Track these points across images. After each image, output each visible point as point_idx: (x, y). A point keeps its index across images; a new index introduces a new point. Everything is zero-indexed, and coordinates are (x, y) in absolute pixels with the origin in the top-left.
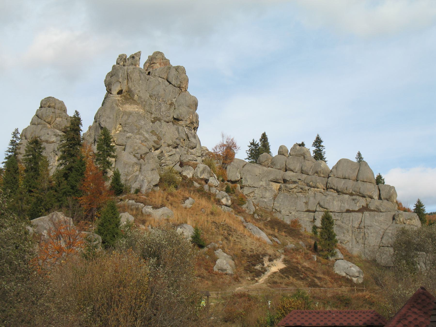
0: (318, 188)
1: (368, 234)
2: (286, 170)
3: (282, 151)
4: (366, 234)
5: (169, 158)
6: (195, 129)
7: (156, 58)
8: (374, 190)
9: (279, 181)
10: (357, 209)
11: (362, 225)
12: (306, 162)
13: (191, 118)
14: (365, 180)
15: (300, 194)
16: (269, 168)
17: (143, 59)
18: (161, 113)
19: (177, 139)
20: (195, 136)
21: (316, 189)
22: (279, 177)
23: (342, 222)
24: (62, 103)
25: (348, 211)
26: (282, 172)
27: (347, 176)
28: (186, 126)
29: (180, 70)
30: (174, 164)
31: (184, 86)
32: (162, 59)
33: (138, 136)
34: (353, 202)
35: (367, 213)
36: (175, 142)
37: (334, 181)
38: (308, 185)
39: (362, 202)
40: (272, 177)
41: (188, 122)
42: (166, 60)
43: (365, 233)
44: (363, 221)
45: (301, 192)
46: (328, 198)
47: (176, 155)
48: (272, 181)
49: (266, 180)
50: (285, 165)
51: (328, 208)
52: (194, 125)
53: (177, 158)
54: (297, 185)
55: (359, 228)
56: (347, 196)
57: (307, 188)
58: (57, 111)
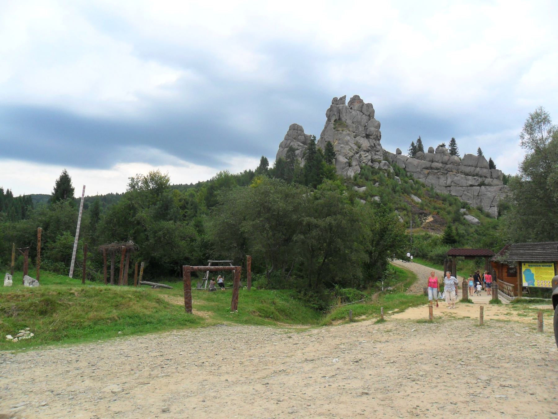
3: (431, 150)
6: (379, 140)
7: (356, 99)
11: (480, 194)
15: (441, 176)
17: (347, 100)
20: (379, 145)
22: (428, 165)
24: (301, 127)
25: (471, 186)
29: (370, 106)
33: (347, 146)
35: (483, 187)
37: (462, 168)
38: (446, 170)
39: (480, 180)
40: (424, 166)
46: (459, 178)
52: (378, 138)
53: (370, 157)
55: (478, 196)
58: (299, 132)
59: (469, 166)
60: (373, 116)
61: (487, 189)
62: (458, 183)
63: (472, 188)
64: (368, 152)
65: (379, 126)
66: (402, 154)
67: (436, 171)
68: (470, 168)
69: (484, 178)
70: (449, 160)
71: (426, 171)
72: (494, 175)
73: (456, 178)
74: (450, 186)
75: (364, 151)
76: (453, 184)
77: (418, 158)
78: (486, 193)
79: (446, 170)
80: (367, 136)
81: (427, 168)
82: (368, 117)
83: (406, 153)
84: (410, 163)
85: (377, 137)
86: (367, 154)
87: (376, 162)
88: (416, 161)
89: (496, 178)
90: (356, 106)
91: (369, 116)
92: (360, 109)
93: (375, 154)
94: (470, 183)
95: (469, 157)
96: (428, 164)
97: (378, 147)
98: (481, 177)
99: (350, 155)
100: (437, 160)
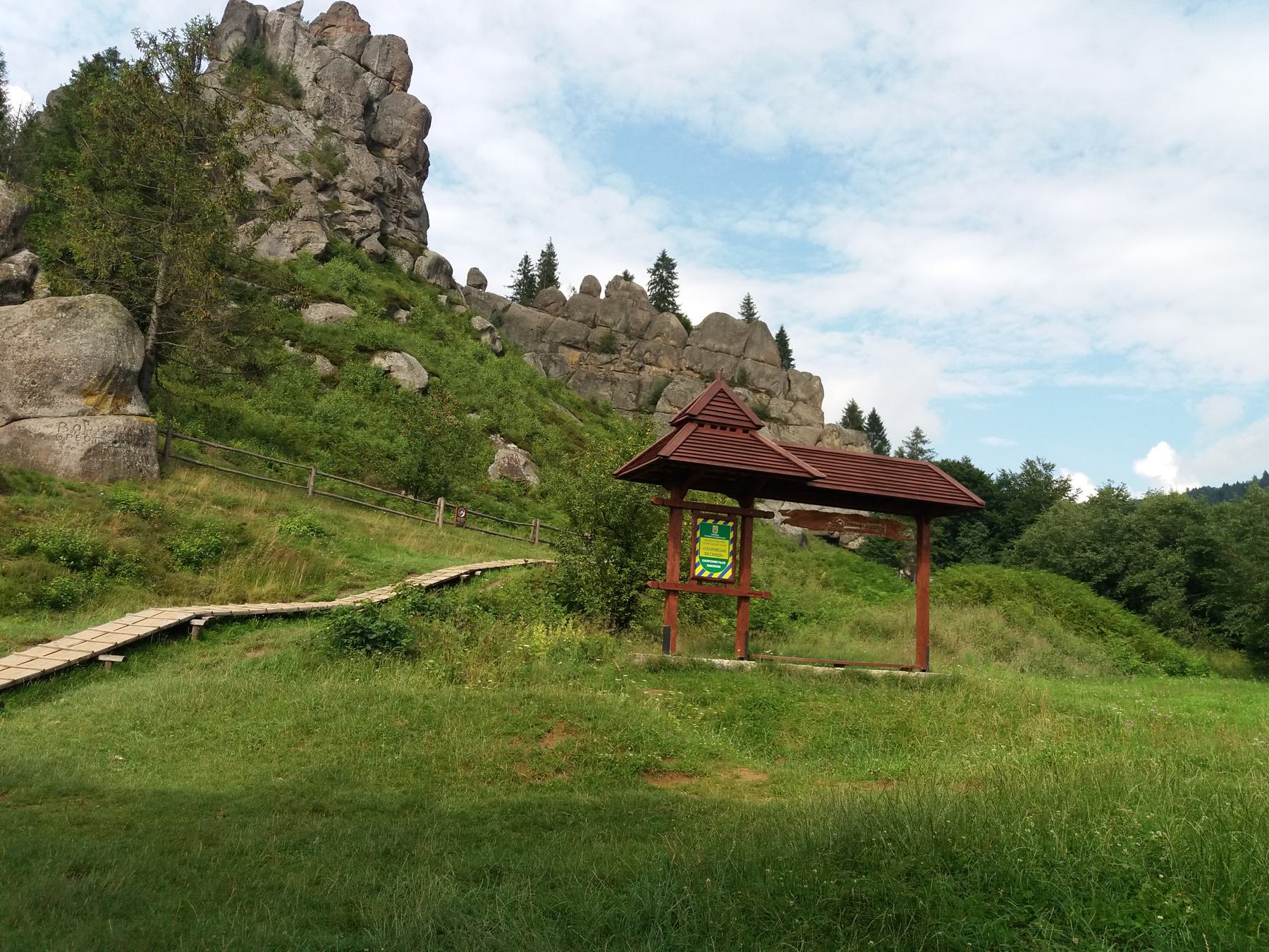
0: (660, 366)
2: (594, 326)
3: (590, 286)
5: (353, 217)
9: (579, 345)
16: (560, 319)
18: (342, 120)
19: (377, 179)
21: (654, 368)
29: (395, 46)
30: (363, 235)
41: (407, 154)
45: (623, 371)
48: (563, 344)
53: (374, 220)
60: (405, 85)
64: (370, 199)
65: (425, 120)
67: (605, 358)
68: (719, 357)
70: (649, 324)
71: (573, 356)
72: (798, 392)
77: (543, 308)
80: (374, 146)
83: (502, 284)
86: (366, 206)
87: (402, 247)
89: (804, 401)
91: (389, 78)
92: (352, 52)
95: (718, 321)
96: (580, 332)
97: (413, 198)
98: (756, 391)
99: (284, 176)
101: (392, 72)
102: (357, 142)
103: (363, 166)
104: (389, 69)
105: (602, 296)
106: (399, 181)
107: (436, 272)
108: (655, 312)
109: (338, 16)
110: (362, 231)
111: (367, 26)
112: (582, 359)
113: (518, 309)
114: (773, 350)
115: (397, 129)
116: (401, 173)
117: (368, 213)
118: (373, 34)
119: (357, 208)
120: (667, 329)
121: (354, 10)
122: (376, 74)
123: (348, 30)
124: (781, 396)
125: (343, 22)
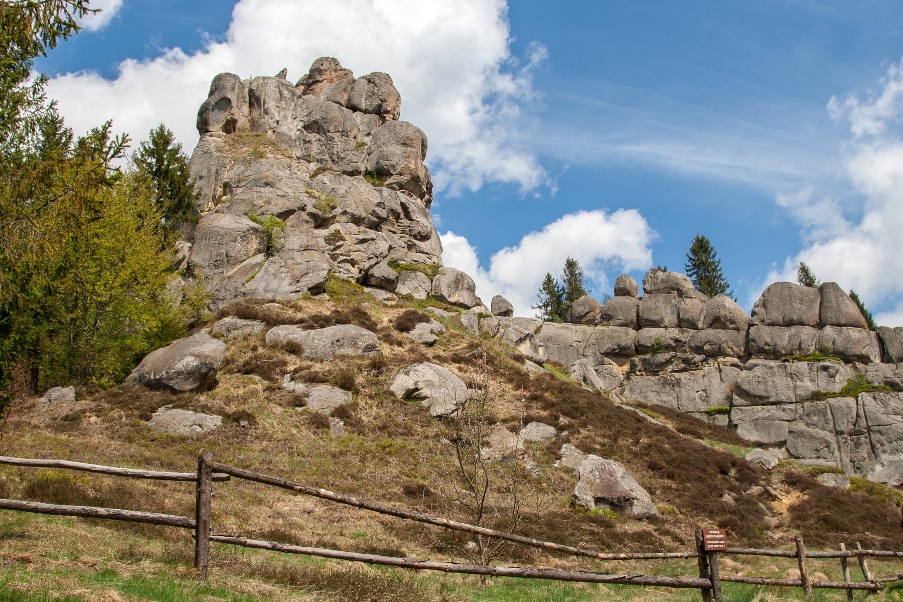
1: (882, 445)
4: (878, 446)
8: (868, 342)
10: (838, 387)
11: (863, 423)
12: (688, 300)
13: (413, 167)
14: (843, 321)
16: (599, 327)
19: (379, 205)
21: (721, 359)
23: (808, 425)
26: (632, 332)
27: (795, 317)
28: (401, 187)
31: (389, 109)
32: (336, 71)
34: (825, 373)
35: (866, 398)
36: (374, 211)
37: (765, 335)
38: (698, 350)
40: (608, 346)
41: (405, 178)
42: (343, 72)
43: (874, 442)
44: (861, 412)
46: (758, 371)
47: (378, 241)
48: (607, 354)
49: (594, 353)
50: (635, 315)
51: (763, 394)
54: (672, 353)
56: (803, 366)
57: (698, 358)
59: (789, 324)
61: (885, 404)
62: (760, 390)
63: (820, 404)
64: (376, 227)
66: (514, 315)
68: (793, 330)
69: (860, 365)
73: (744, 373)
74: (727, 412)
75: (357, 220)
76: (737, 400)
77: (577, 320)
78: (884, 419)
79: (698, 350)
81: (619, 354)
82: (375, 117)
84: (549, 339)
85: (415, 179)
86: (372, 234)
88: (572, 333)
90: (324, 89)
93: (410, 247)
94: (808, 386)
100: (655, 318)
101: (380, 106)
102: (352, 174)
103: (363, 195)
104: (377, 102)
105: (641, 293)
106: (403, 205)
107: (457, 288)
108: (705, 297)
109: (320, 72)
110: (369, 258)
111: (347, 73)
112: (633, 366)
113: (554, 329)
114: (852, 309)
115: (394, 154)
116: (403, 197)
117: (373, 239)
118: (356, 76)
119: (361, 237)
120: (723, 313)
121: (334, 60)
122: (366, 112)
123: (331, 81)
124: (877, 360)
125: (327, 75)
